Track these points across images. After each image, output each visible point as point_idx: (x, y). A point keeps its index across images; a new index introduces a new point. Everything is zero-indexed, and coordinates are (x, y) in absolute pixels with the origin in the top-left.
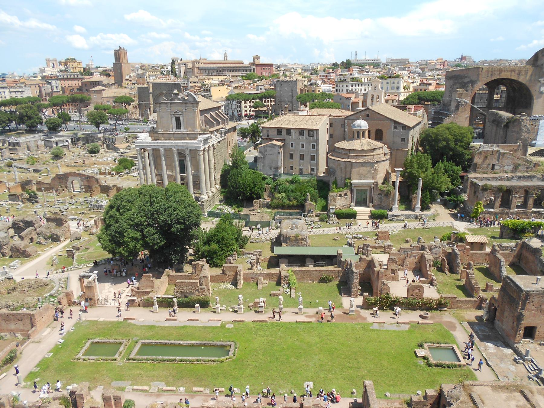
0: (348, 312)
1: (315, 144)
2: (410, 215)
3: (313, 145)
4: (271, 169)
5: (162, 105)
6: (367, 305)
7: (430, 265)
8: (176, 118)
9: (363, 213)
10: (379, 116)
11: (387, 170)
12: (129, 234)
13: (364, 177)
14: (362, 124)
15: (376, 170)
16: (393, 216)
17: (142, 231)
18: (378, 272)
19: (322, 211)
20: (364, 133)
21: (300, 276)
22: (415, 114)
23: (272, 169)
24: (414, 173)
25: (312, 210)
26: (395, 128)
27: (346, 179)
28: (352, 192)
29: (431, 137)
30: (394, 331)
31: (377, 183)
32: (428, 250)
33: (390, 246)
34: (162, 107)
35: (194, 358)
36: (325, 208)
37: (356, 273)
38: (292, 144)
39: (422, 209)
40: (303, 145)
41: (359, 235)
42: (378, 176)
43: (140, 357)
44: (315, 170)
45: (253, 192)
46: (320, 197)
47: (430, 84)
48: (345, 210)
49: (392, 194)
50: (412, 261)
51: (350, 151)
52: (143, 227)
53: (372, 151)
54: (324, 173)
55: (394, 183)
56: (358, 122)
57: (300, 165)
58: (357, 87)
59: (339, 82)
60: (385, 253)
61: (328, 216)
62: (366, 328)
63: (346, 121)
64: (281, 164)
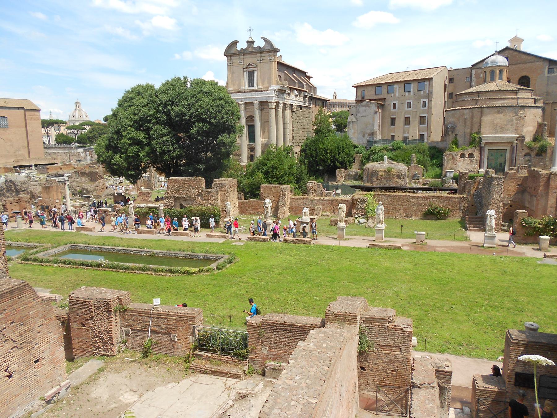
1: (427, 100)
3: (424, 102)
4: (364, 136)
5: (233, 58)
12: (129, 134)
13: (503, 129)
15: (521, 119)
17: (147, 131)
20: (501, 72)
23: (366, 136)
28: (481, 150)
34: (234, 61)
35: (137, 265)
38: (395, 104)
40: (409, 104)
45: (337, 160)
52: (151, 125)
57: (404, 132)
63: (473, 72)
64: (377, 128)
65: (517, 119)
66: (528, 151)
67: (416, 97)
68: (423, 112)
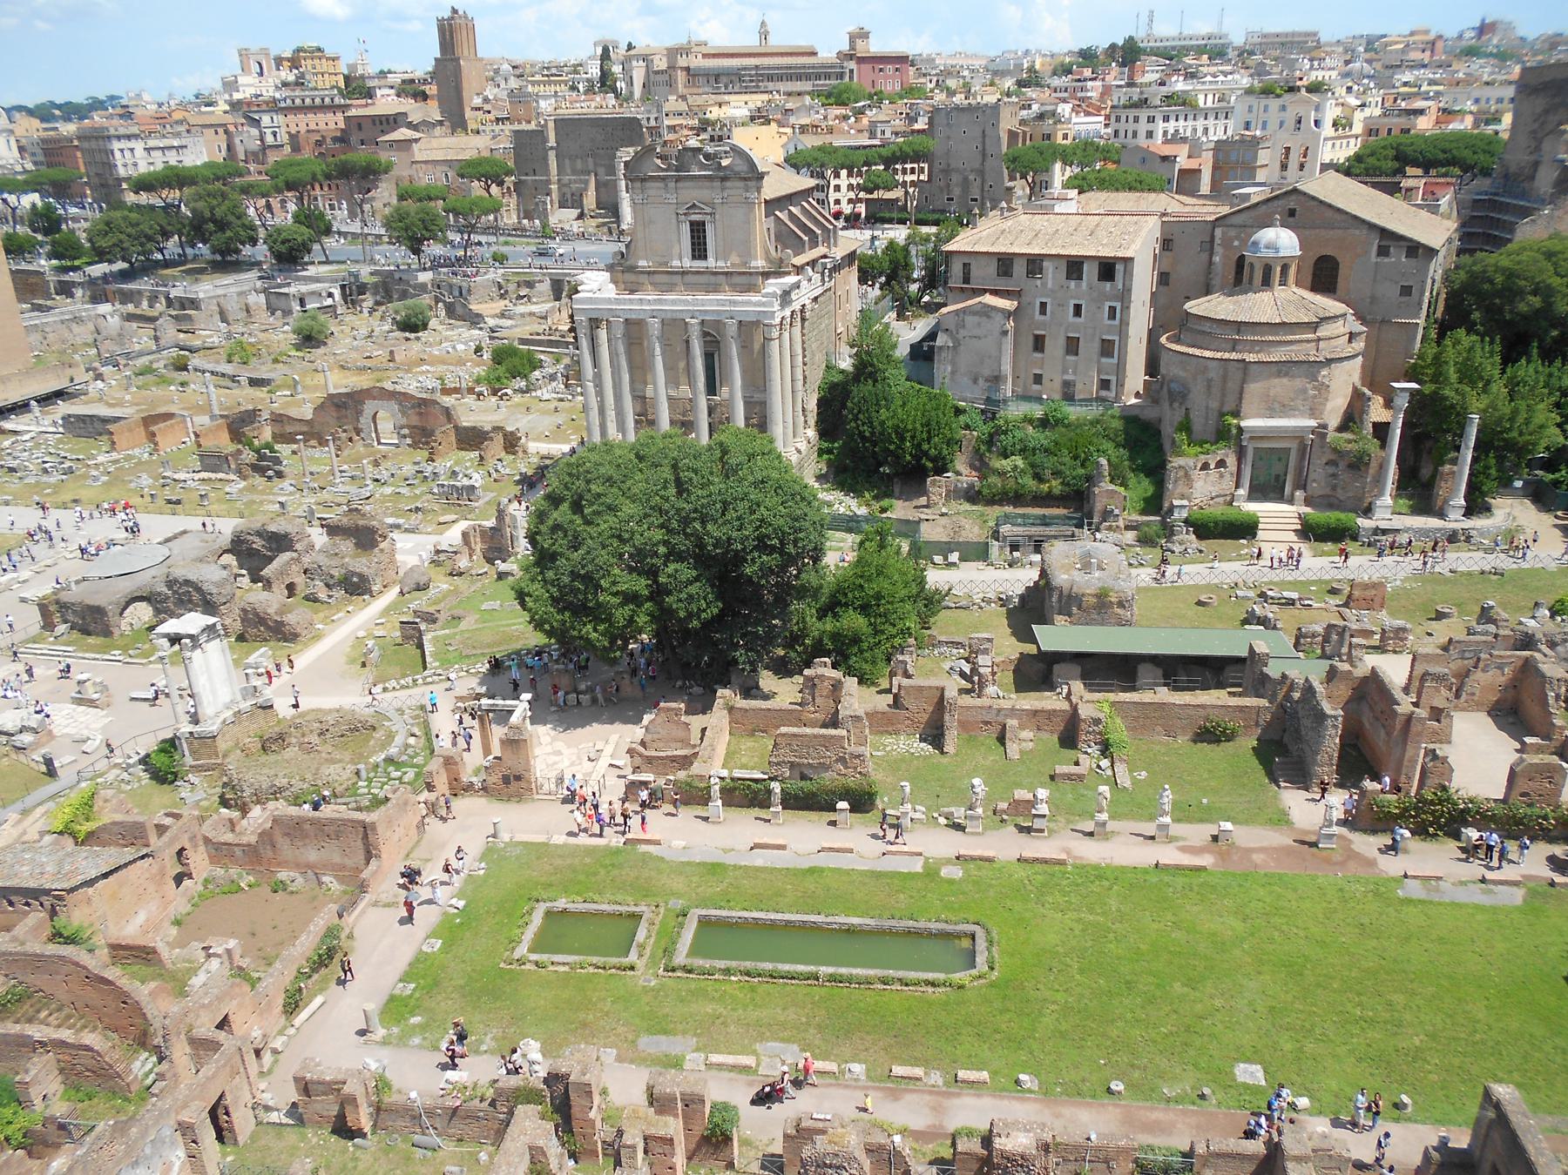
0: (1313, 839)
1: (1118, 305)
2: (1429, 530)
3: (1112, 310)
4: (975, 381)
5: (648, 184)
6: (1366, 819)
7: (1558, 697)
8: (692, 223)
9: (1278, 518)
10: (1329, 214)
11: (1355, 389)
12: (614, 583)
13: (1285, 410)
14: (1282, 240)
15: (1323, 388)
16: (1377, 531)
17: (653, 573)
18: (1409, 718)
19: (1144, 512)
20: (1285, 268)
21: (1136, 719)
22: (1434, 209)
23: (981, 381)
24: (1446, 398)
25: (1117, 512)
26: (1383, 252)
27: (1222, 415)
28: (1241, 454)
29: (1491, 282)
30: (1477, 907)
31: (1325, 427)
32: (1543, 647)
33: (1404, 630)
34: (651, 192)
35: (871, 972)
36: (1154, 504)
37: (1336, 717)
38: (1043, 305)
39: (1469, 512)
40: (1078, 308)
41: (1286, 594)
42: (1329, 406)
43: (699, 962)
44: (1113, 386)
45: (926, 454)
46: (1133, 471)
47: (1421, 112)
48: (1218, 511)
49: (1374, 465)
50: (1489, 681)
51: (1239, 326)
52: (658, 562)
53: (1313, 326)
54: (1137, 395)
55: (1381, 430)
56: (1268, 235)
57: (1065, 372)
58: (1181, 122)
59: (1125, 107)
60: (1385, 652)
61: (1168, 531)
62: (1382, 890)
63: (1218, 232)
64: (1007, 368)
65: (1315, 388)
66: (1333, 457)
67: (1095, 295)
68: (1110, 330)
